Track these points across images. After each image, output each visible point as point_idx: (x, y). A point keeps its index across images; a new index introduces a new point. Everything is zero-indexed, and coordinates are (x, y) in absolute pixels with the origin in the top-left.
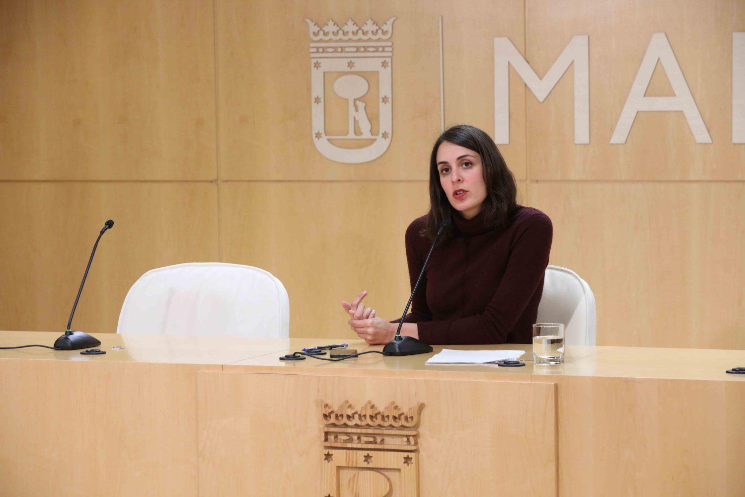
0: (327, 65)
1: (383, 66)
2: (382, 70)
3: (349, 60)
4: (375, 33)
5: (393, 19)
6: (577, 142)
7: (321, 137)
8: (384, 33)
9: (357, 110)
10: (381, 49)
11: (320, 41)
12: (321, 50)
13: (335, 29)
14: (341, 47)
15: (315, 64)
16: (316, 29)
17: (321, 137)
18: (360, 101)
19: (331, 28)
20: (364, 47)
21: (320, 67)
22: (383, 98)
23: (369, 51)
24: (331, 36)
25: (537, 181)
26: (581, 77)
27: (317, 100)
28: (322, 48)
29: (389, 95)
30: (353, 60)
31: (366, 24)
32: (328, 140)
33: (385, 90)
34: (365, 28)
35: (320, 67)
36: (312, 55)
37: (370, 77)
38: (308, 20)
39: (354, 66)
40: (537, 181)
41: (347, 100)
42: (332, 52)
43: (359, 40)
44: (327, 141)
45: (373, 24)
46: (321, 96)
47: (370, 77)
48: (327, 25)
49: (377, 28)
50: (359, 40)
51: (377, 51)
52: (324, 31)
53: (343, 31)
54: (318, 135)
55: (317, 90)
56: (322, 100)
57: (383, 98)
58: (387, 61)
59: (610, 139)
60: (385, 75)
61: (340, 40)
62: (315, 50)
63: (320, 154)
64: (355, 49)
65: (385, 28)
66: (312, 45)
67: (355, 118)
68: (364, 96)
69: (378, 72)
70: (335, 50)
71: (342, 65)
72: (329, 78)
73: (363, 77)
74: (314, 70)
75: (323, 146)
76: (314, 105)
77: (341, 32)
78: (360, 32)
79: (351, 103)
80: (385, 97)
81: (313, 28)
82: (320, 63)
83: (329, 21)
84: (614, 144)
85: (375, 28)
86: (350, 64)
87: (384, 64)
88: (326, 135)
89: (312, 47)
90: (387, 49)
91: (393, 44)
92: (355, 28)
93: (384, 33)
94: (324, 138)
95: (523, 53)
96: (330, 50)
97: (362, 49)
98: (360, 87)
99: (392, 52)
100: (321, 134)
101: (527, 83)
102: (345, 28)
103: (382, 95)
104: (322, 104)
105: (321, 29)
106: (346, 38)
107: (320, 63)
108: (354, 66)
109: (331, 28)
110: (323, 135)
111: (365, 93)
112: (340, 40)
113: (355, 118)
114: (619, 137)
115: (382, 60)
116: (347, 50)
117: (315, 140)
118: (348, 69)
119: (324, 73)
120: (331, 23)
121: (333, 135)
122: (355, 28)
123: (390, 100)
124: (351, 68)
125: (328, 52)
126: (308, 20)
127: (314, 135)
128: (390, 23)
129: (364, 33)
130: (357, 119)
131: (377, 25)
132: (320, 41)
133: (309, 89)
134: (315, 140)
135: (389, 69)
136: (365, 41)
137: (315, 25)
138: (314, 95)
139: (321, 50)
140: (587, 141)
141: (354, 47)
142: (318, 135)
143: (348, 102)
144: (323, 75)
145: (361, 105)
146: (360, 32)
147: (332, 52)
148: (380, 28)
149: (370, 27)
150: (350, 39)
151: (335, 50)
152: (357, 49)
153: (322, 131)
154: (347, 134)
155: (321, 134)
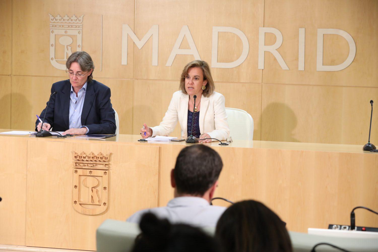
0: (56, 32)
1: (78, 33)
2: (78, 35)
3: (65, 30)
4: (76, 20)
5: (83, 16)
7: (53, 60)
8: (79, 20)
9: (68, 50)
10: (78, 27)
11: (54, 22)
12: (54, 26)
13: (60, 18)
14: (62, 25)
15: (52, 31)
16: (53, 18)
17: (53, 60)
18: (69, 46)
19: (58, 18)
20: (71, 26)
21: (54, 32)
22: (78, 46)
23: (73, 27)
24: (58, 21)
25: (137, 79)
27: (52, 45)
28: (55, 25)
29: (81, 44)
30: (67, 30)
31: (73, 17)
32: (56, 61)
33: (79, 43)
34: (72, 18)
35: (54, 32)
36: (51, 28)
37: (73, 37)
38: (49, 14)
39: (67, 33)
41: (64, 46)
42: (58, 27)
43: (70, 23)
44: (56, 62)
45: (75, 17)
46: (54, 44)
47: (73, 37)
48: (57, 16)
49: (77, 19)
50: (70, 23)
51: (76, 27)
52: (56, 19)
53: (63, 19)
54: (52, 59)
55: (52, 41)
56: (54, 45)
57: (78, 46)
58: (80, 31)
60: (79, 37)
61: (62, 23)
62: (52, 26)
63: (53, 66)
64: (68, 26)
65: (80, 19)
66: (51, 24)
67: (67, 53)
68: (70, 45)
69: (77, 35)
70: (60, 26)
71: (63, 32)
72: (57, 37)
73: (70, 37)
74: (51, 34)
75: (54, 63)
76: (51, 47)
77: (62, 19)
78: (70, 20)
79: (66, 47)
80: (79, 45)
81: (51, 18)
82: (54, 31)
83: (58, 15)
85: (76, 18)
86: (66, 32)
87: (79, 33)
88: (55, 59)
89: (51, 25)
90: (80, 27)
91: (83, 25)
92: (68, 18)
93: (79, 20)
94: (54, 60)
96: (58, 26)
97: (71, 26)
98: (69, 41)
99: (82, 28)
100: (53, 58)
102: (64, 18)
103: (78, 44)
104: (54, 47)
105: (54, 18)
106: (64, 22)
107: (54, 31)
108: (67, 33)
109: (58, 18)
110: (54, 59)
111: (71, 43)
112: (62, 23)
113: (67, 53)
115: (79, 31)
116: (65, 26)
117: (51, 61)
118: (65, 34)
119: (55, 35)
120: (59, 16)
121: (57, 59)
122: (68, 18)
123: (81, 46)
124: (66, 33)
125: (57, 27)
126: (49, 14)
127: (50, 59)
128: (82, 17)
129: (71, 20)
130: (68, 53)
131: (77, 17)
132: (54, 22)
133: (49, 41)
134: (51, 61)
135: (81, 34)
136: (72, 23)
137: (52, 16)
138: (51, 43)
139: (54, 26)
141: (68, 25)
142: (52, 59)
143: (64, 47)
144: (55, 36)
145: (69, 48)
146: (70, 20)
147: (58, 27)
148: (78, 19)
149: (74, 18)
150: (66, 22)
151: (60, 26)
152: (69, 27)
153: (54, 57)
154: (64, 59)
155: (53, 58)
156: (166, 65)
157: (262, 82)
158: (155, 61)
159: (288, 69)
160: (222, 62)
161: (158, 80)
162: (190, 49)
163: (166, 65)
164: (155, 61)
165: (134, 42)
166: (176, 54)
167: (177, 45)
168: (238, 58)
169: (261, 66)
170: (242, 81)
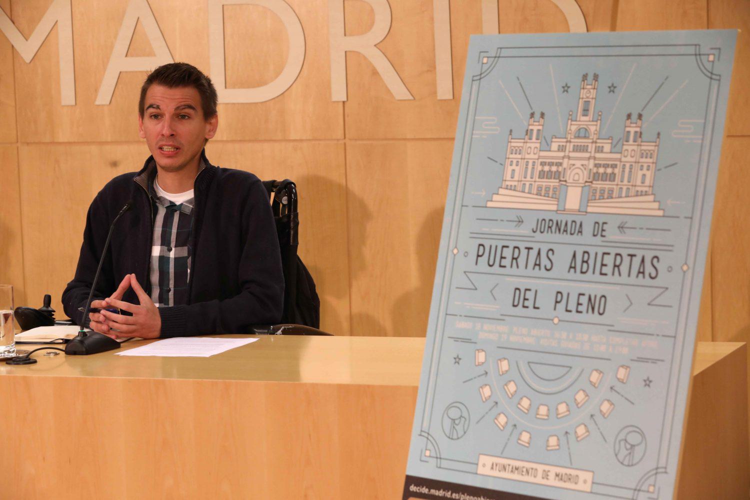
6: (63, 103)
26: (64, 35)
40: (28, 144)
59: (95, 100)
84: (98, 106)
95: (10, 16)
101: (13, 44)
114: (103, 97)
140: (73, 103)
156: (97, 103)
157: (345, 138)
158: (67, 95)
159: (411, 98)
160: (239, 88)
161: (78, 143)
162: (155, 55)
163: (97, 103)
164: (67, 95)
165: (13, 46)
166: (120, 72)
167: (121, 46)
168: (278, 74)
169: (338, 93)
170: (293, 137)
